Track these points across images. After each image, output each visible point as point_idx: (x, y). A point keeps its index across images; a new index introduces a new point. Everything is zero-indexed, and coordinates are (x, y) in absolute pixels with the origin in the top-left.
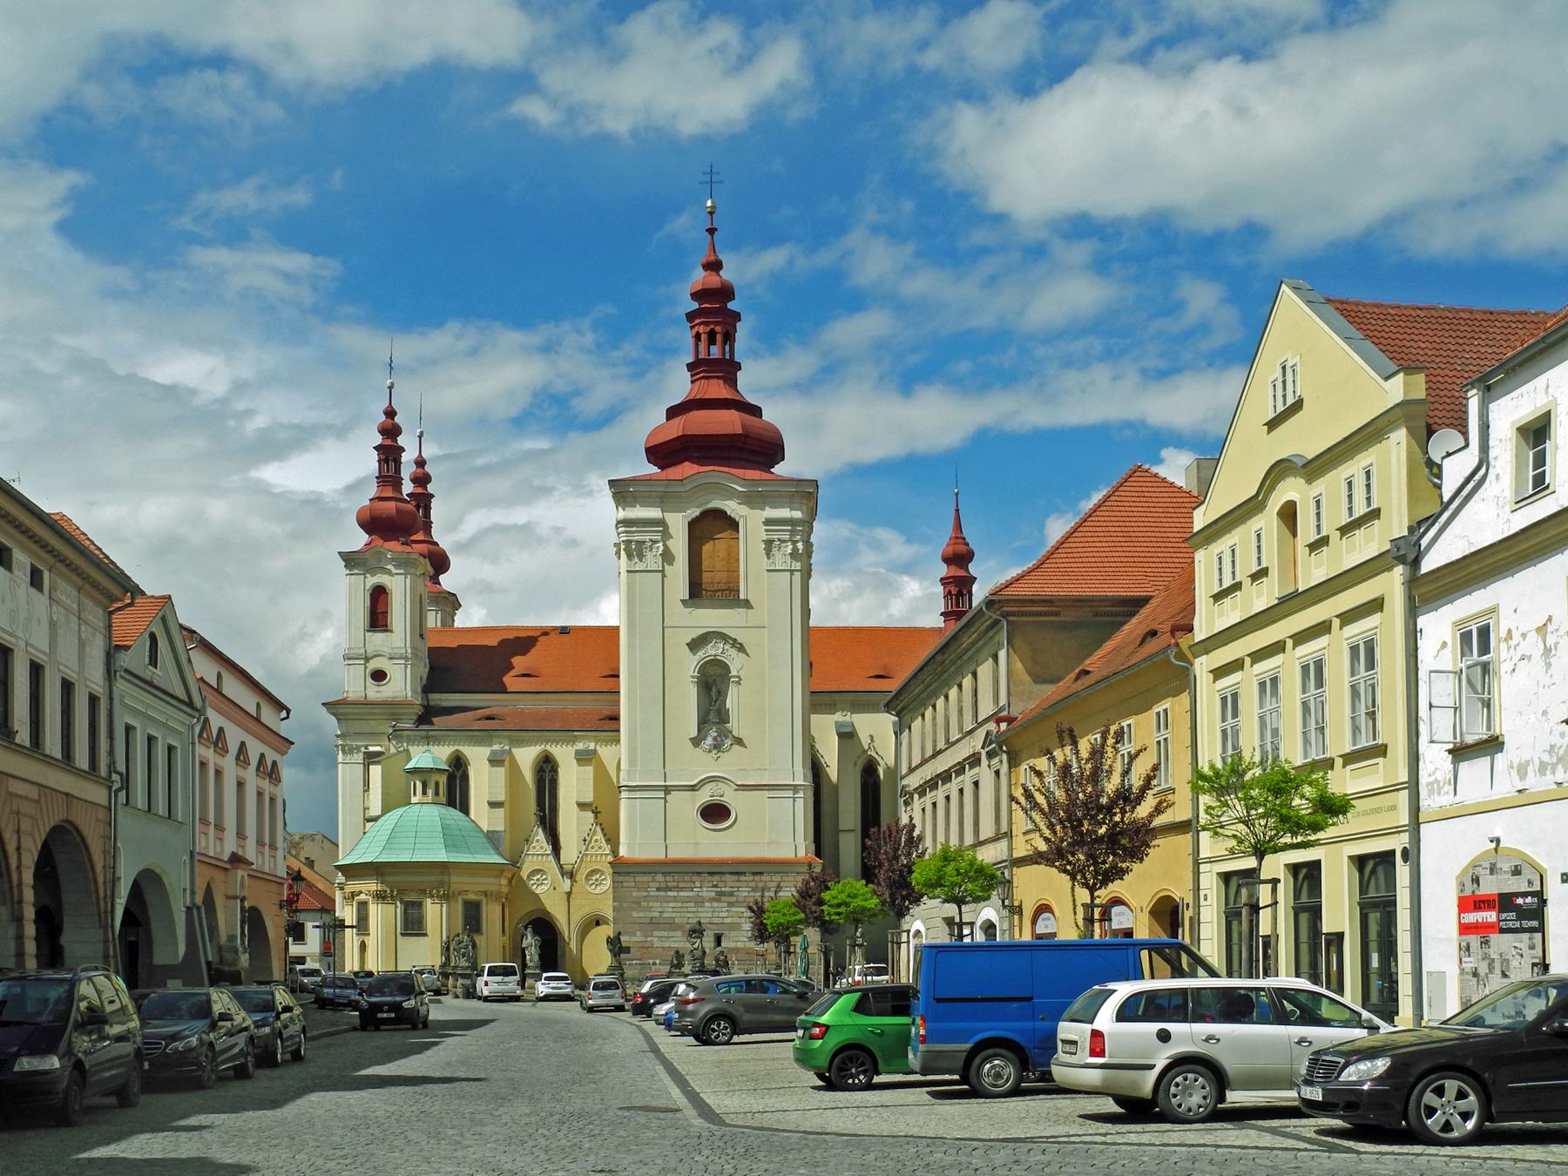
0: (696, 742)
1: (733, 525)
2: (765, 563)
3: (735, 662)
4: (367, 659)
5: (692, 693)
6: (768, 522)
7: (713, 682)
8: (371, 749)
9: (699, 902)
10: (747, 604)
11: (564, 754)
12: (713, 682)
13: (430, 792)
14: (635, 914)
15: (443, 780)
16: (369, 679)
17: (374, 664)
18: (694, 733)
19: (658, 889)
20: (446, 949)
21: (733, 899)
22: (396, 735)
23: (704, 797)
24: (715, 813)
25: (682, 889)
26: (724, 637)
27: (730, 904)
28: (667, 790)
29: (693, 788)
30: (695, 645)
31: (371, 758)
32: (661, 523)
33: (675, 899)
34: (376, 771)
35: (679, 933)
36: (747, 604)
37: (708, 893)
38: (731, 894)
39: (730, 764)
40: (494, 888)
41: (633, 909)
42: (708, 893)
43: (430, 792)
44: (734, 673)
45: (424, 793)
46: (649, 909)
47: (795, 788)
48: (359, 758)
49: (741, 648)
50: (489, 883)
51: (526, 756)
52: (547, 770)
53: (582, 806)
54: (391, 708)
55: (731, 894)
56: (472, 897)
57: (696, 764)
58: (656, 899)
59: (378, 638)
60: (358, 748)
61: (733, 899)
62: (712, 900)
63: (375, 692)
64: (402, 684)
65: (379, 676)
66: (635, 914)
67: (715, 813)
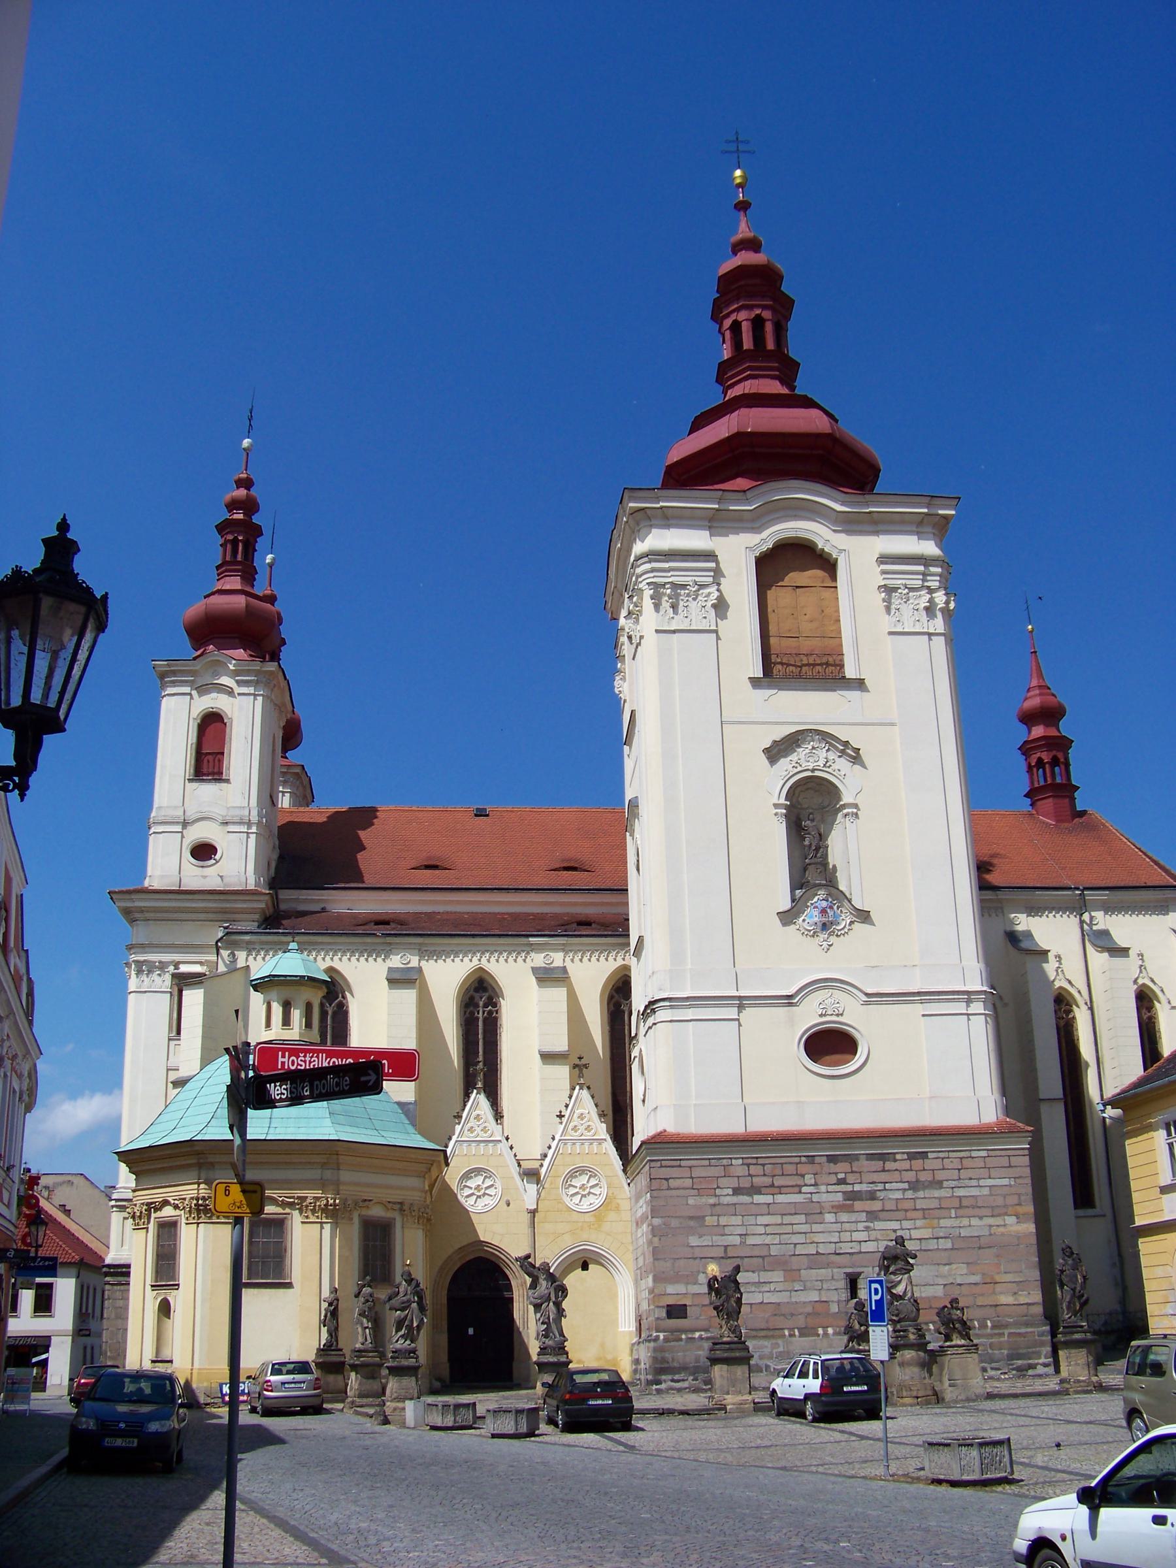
0: (787, 917)
1: (828, 565)
2: (886, 623)
3: (851, 783)
4: (185, 824)
5: (779, 832)
6: (884, 559)
7: (810, 813)
8: (184, 968)
9: (813, 1212)
10: (859, 684)
11: (513, 972)
12: (810, 813)
13: (296, 1015)
14: (694, 1241)
15: (316, 997)
16: (187, 855)
17: (198, 833)
18: (786, 904)
19: (737, 1191)
20: (332, 1315)
21: (876, 1206)
22: (230, 940)
23: (809, 1016)
24: (830, 1045)
25: (780, 1190)
26: (826, 737)
27: (872, 1216)
28: (741, 1003)
29: (788, 1000)
30: (775, 752)
31: (183, 981)
32: (710, 556)
33: (769, 1209)
34: (194, 999)
35: (777, 1276)
36: (860, 684)
37: (831, 1195)
38: (872, 1196)
39: (852, 955)
40: (414, 1196)
41: (691, 1231)
42: (831, 1195)
43: (296, 1015)
44: (846, 798)
45: (286, 1022)
46: (721, 1230)
47: (969, 997)
48: (164, 982)
49: (856, 758)
50: (409, 1187)
51: (446, 975)
52: (480, 998)
53: (548, 1057)
54: (219, 902)
55: (872, 1196)
56: (376, 1212)
57: (791, 955)
58: (733, 1210)
59: (207, 790)
60: (163, 966)
61: (876, 1206)
62: (838, 1209)
63: (198, 877)
64: (239, 864)
65: (204, 852)
66: (694, 1241)
67: (830, 1045)
